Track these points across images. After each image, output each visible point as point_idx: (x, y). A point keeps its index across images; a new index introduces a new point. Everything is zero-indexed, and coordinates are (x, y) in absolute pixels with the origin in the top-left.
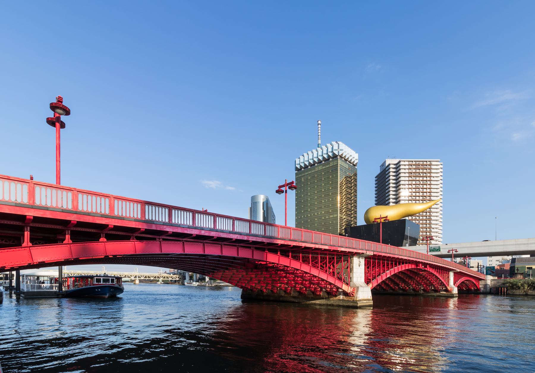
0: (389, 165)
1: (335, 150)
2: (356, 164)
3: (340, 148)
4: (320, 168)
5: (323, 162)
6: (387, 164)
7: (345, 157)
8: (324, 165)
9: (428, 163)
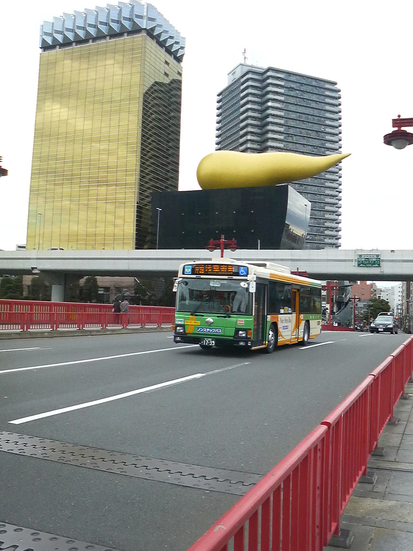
1: (138, 17)
7: (159, 35)
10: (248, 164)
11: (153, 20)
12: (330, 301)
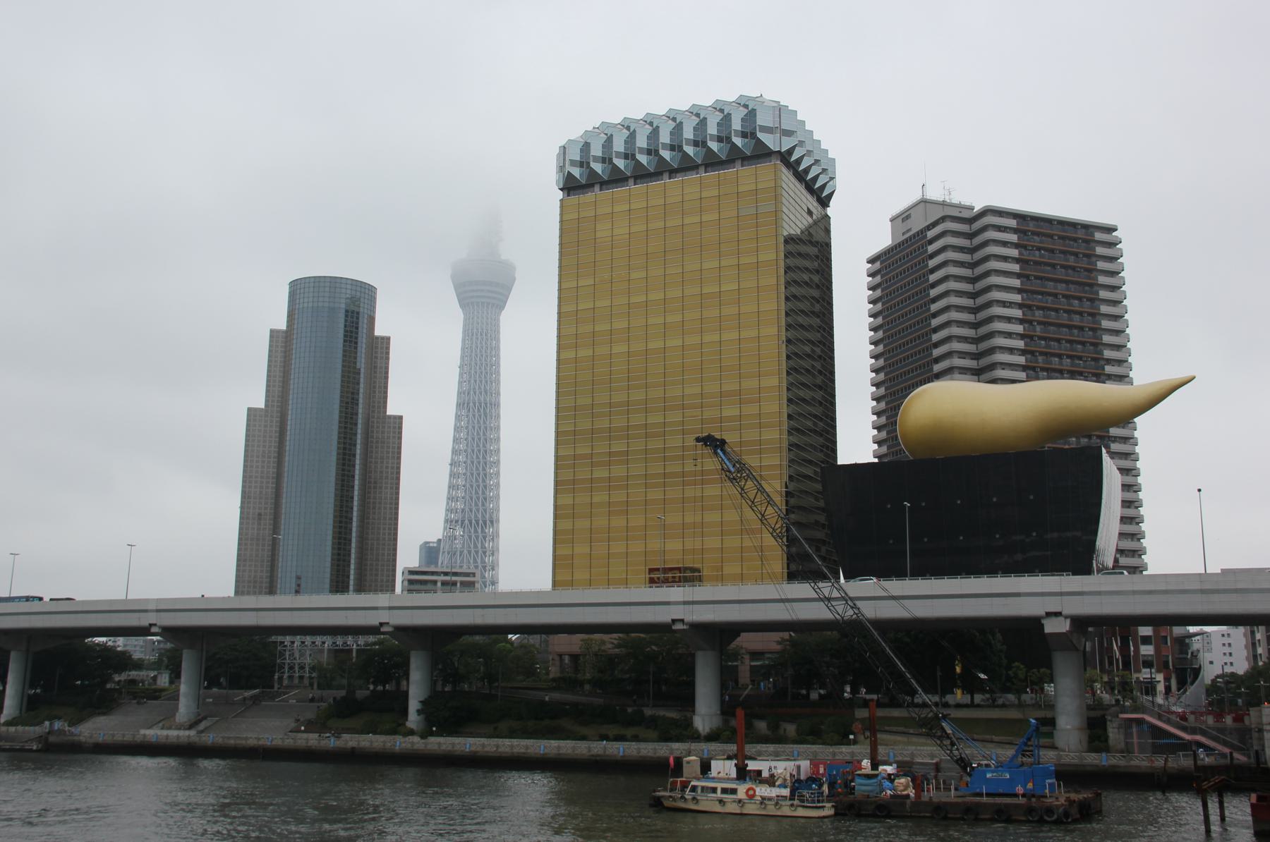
0: (943, 219)
7: (799, 161)
9: (1080, 234)
10: (960, 403)
11: (788, 133)
12: (1164, 667)
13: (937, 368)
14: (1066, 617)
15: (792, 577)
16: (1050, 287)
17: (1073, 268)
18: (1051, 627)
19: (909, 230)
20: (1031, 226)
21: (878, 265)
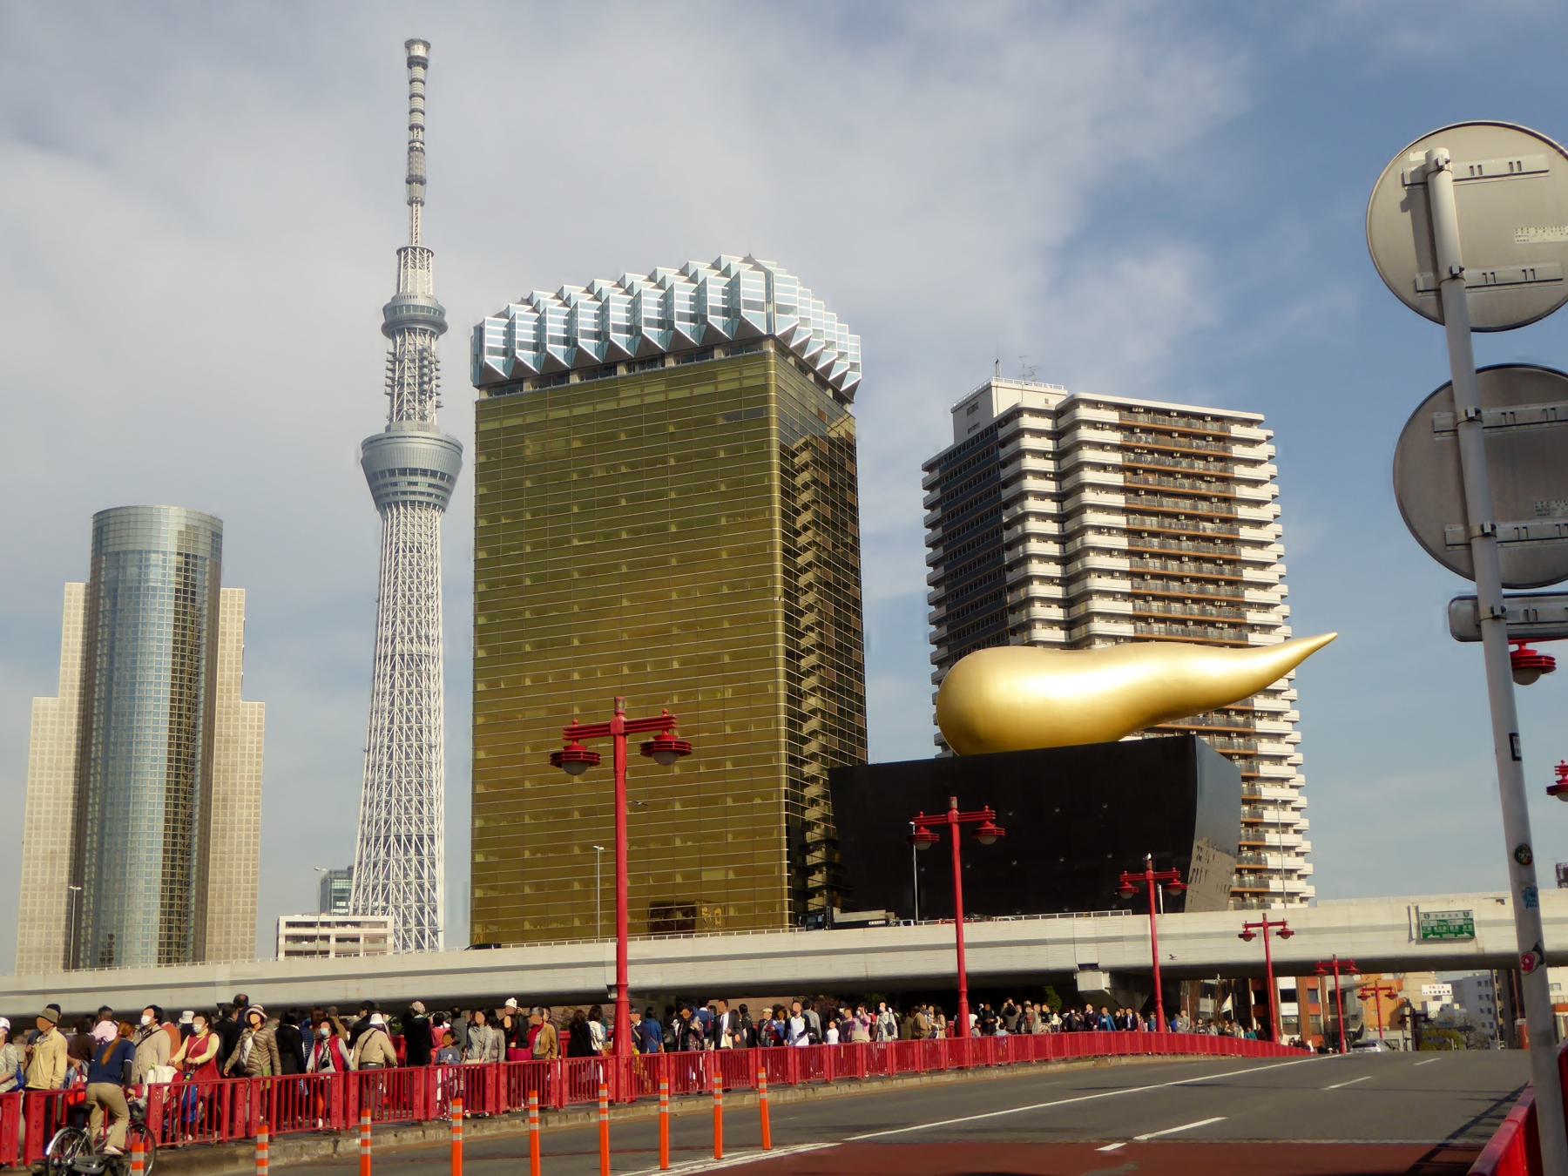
0: (1016, 412)
1: (752, 305)
2: (853, 389)
3: (780, 296)
4: (655, 392)
5: (670, 363)
6: (1001, 404)
7: (803, 346)
8: (673, 380)
9: (1212, 428)
13: (1013, 620)
14: (1104, 970)
15: (804, 919)
16: (1168, 504)
17: (1201, 477)
18: (1085, 982)
19: (976, 426)
20: (1143, 420)
21: (936, 474)
